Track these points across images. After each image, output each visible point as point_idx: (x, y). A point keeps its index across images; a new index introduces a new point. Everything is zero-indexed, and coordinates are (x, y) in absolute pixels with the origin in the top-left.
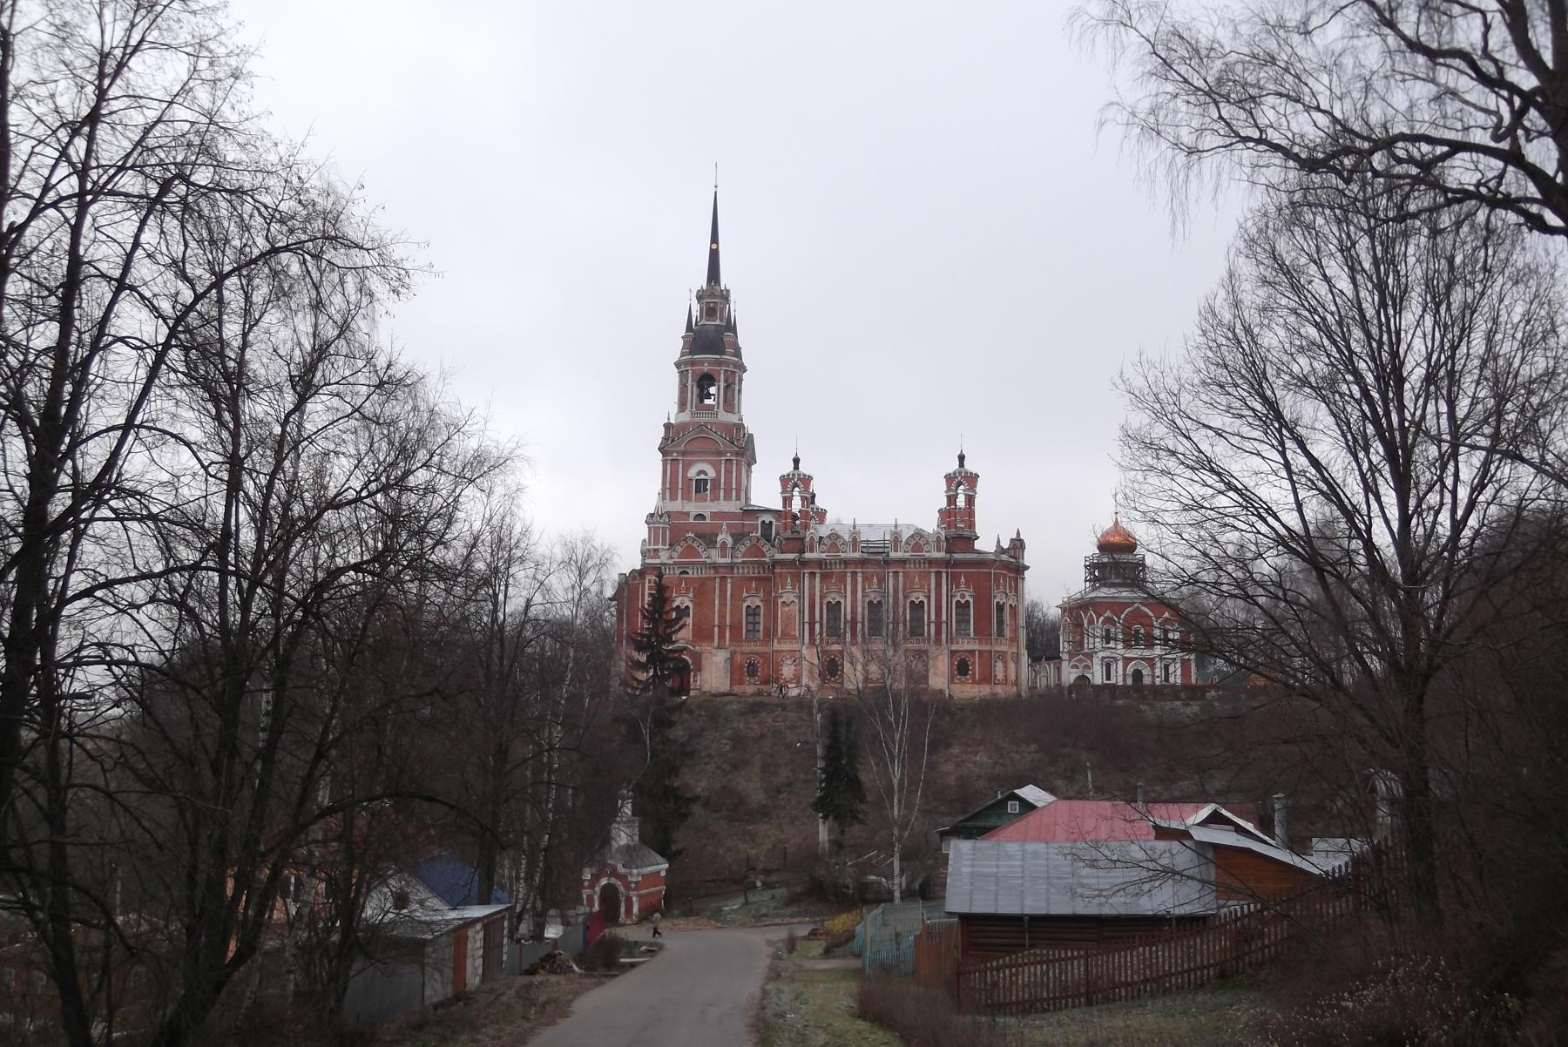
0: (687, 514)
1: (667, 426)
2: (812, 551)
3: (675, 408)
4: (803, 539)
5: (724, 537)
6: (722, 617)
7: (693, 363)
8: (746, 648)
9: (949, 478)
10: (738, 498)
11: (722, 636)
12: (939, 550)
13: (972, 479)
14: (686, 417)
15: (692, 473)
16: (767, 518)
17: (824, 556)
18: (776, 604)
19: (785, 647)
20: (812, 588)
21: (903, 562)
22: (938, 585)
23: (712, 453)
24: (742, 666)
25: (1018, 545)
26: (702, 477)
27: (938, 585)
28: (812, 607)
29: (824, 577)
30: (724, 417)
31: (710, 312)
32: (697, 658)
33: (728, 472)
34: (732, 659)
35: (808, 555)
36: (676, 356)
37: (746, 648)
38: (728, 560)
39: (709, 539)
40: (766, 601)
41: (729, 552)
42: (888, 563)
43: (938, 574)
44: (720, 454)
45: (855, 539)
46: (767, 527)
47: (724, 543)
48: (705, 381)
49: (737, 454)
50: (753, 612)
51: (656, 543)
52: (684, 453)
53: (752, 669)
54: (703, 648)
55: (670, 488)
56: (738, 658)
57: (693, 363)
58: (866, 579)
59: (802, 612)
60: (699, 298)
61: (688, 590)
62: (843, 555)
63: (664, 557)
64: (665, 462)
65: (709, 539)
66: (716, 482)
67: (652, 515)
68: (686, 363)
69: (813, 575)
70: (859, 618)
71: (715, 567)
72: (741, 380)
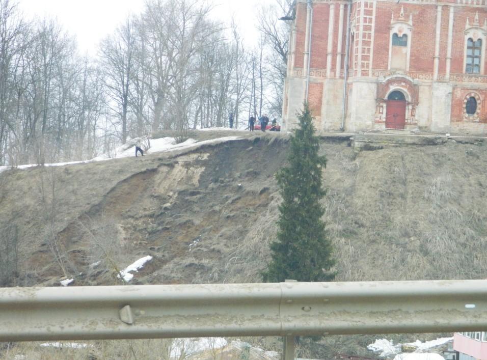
6: (443, 48)
8: (468, 83)
11: (442, 69)
24: (461, 101)
32: (414, 89)
53: (471, 106)
54: (421, 80)
61: (407, 17)
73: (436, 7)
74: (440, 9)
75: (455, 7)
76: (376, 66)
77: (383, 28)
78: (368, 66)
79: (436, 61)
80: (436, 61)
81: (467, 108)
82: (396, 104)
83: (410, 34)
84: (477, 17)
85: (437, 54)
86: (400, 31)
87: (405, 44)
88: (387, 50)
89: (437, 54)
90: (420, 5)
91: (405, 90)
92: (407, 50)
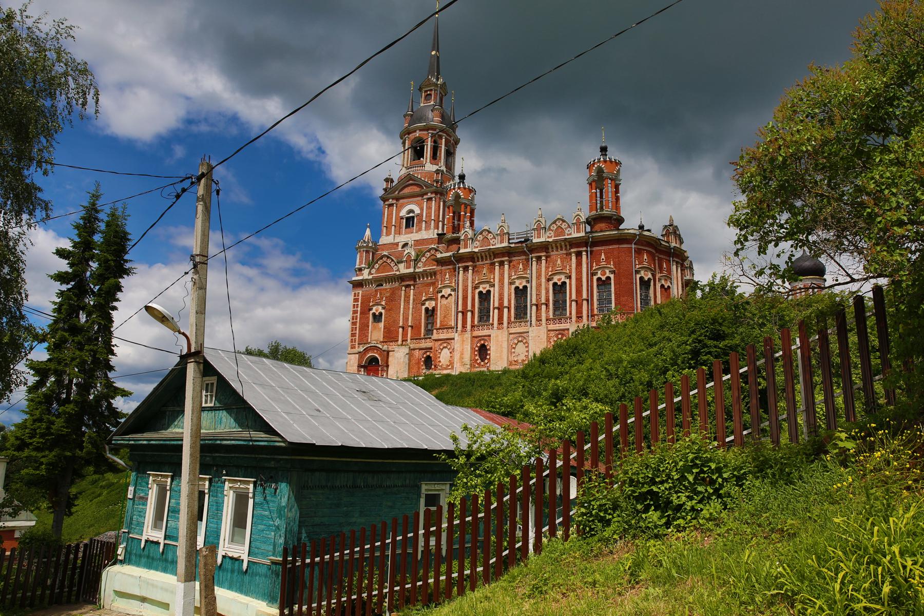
0: (397, 244)
2: (466, 247)
6: (406, 319)
12: (578, 231)
15: (403, 213)
20: (465, 280)
22: (579, 264)
26: (411, 215)
27: (579, 264)
28: (465, 298)
33: (429, 208)
34: (410, 355)
38: (411, 270)
43: (579, 255)
54: (392, 346)
66: (420, 216)
70: (506, 304)
71: (402, 278)
85: (401, 324)
89: (401, 324)
92: (382, 325)
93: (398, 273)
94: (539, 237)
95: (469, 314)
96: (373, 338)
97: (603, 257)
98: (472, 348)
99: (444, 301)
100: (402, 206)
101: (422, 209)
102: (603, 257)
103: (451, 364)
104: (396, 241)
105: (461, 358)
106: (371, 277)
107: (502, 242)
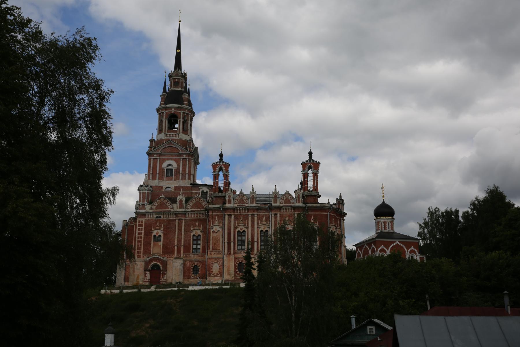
0: (161, 187)
1: (152, 141)
2: (229, 203)
3: (156, 132)
4: (224, 197)
5: (181, 198)
6: (179, 241)
7: (166, 109)
8: (192, 258)
9: (304, 164)
10: (189, 179)
11: (179, 251)
12: (299, 202)
13: (317, 165)
14: (162, 136)
15: (165, 165)
16: (205, 189)
17: (236, 205)
18: (209, 233)
19: (214, 256)
20: (229, 223)
21: (280, 208)
23: (176, 155)
24: (189, 268)
25: (340, 202)
26: (170, 167)
29: (236, 217)
30: (183, 137)
31: (176, 83)
32: (165, 264)
33: (184, 165)
34: (184, 264)
35: (227, 205)
36: (158, 105)
37: (192, 258)
38: (183, 210)
39: (173, 200)
40: (204, 232)
41: (184, 205)
42: (271, 209)
44: (180, 155)
45: (253, 196)
46: (205, 194)
47: (181, 201)
48: (173, 120)
49: (189, 155)
50: (197, 239)
51: (143, 201)
52: (160, 155)
53: (195, 269)
54: (170, 258)
55: (152, 173)
56: (188, 264)
57: (166, 109)
58: (259, 218)
59: (224, 236)
60: (170, 76)
61: (160, 226)
62: (246, 205)
63: (148, 208)
64: (150, 160)
65: (173, 200)
67: (141, 186)
68: (162, 109)
69: (230, 216)
70: (256, 240)
71: (176, 214)
72: (192, 120)
73: (176, 220)
74: (177, 221)
75: (185, 219)
76: (145, 253)
77: (148, 232)
78: (140, 253)
79: (176, 248)
80: (176, 248)
81: (193, 271)
82: (156, 271)
83: (162, 234)
84: (197, 224)
85: (176, 244)
86: (157, 234)
87: (160, 241)
88: (151, 244)
89: (176, 244)
90: (167, 220)
91: (159, 264)
93: (172, 210)
94: (276, 203)
95: (232, 244)
96: (155, 252)
97: (312, 218)
98: (235, 265)
99: (215, 235)
100: (164, 160)
101: (179, 165)
102: (312, 218)
103: (221, 274)
104: (161, 185)
105: (228, 270)
106: (151, 211)
107: (253, 203)
